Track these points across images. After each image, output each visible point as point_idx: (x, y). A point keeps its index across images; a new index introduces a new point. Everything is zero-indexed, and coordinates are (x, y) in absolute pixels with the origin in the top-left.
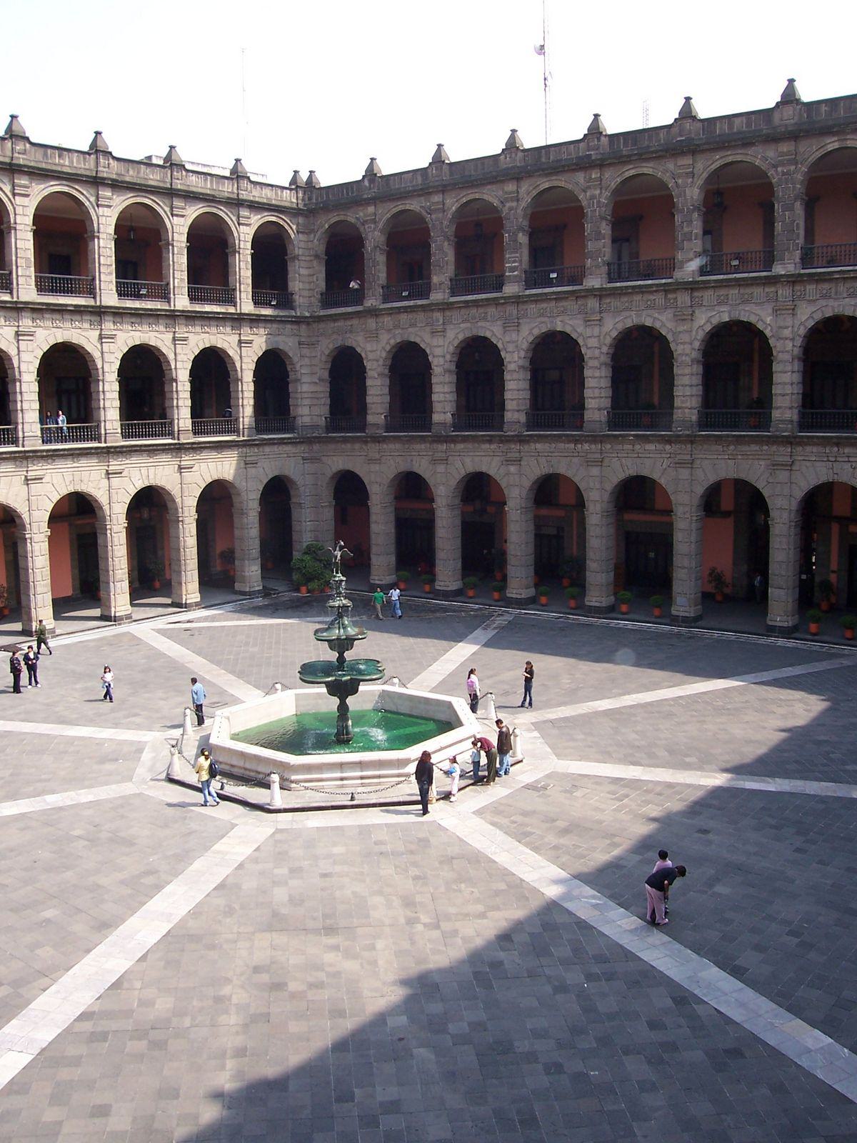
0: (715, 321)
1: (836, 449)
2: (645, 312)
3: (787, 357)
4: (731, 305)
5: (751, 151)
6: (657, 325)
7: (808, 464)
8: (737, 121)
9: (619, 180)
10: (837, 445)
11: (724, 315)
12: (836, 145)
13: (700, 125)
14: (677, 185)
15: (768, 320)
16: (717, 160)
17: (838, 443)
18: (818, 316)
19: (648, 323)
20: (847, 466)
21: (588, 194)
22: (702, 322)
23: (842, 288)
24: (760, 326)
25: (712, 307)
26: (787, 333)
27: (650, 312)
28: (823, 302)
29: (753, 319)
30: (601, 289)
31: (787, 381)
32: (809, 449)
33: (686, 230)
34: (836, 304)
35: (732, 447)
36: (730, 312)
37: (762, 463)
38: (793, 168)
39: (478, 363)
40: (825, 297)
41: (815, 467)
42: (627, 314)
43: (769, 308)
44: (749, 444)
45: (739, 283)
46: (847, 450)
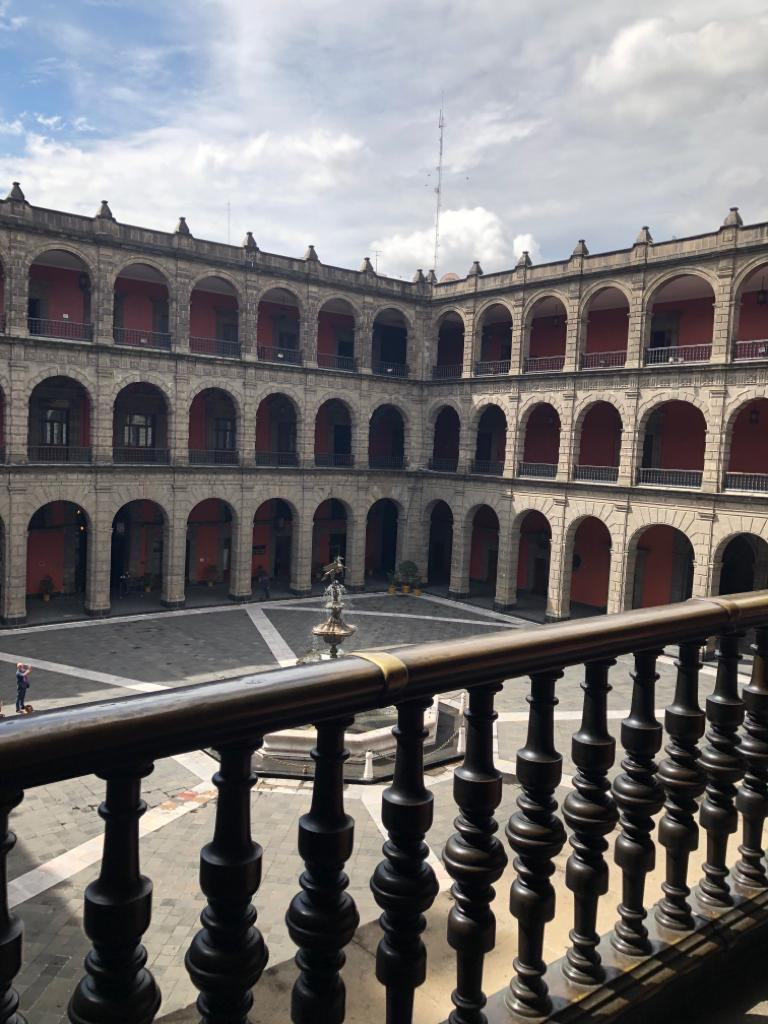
0: (130, 381)
1: (214, 476)
2: (68, 367)
3: (183, 412)
4: (141, 371)
5: (158, 260)
6: (80, 378)
7: (197, 487)
8: (147, 235)
9: (44, 249)
10: (215, 473)
11: (136, 377)
12: (214, 274)
13: (117, 227)
14: (99, 269)
15: (170, 385)
16: (132, 259)
17: (215, 472)
18: (203, 387)
19: (72, 375)
20: (221, 487)
21: (13, 252)
22: (119, 380)
23: (219, 369)
24: (163, 389)
25: (126, 370)
26: (184, 396)
27: (73, 367)
28: (207, 378)
29: (159, 383)
30: (26, 340)
31: (180, 427)
32: (197, 476)
33: (106, 306)
34: (214, 380)
35: (143, 476)
36: (140, 376)
37: (165, 487)
38: (187, 281)
39: (389, 423)
40: (207, 374)
41: (200, 489)
42: (49, 365)
43: (170, 377)
44: (155, 473)
45: (150, 355)
46: (223, 477)
